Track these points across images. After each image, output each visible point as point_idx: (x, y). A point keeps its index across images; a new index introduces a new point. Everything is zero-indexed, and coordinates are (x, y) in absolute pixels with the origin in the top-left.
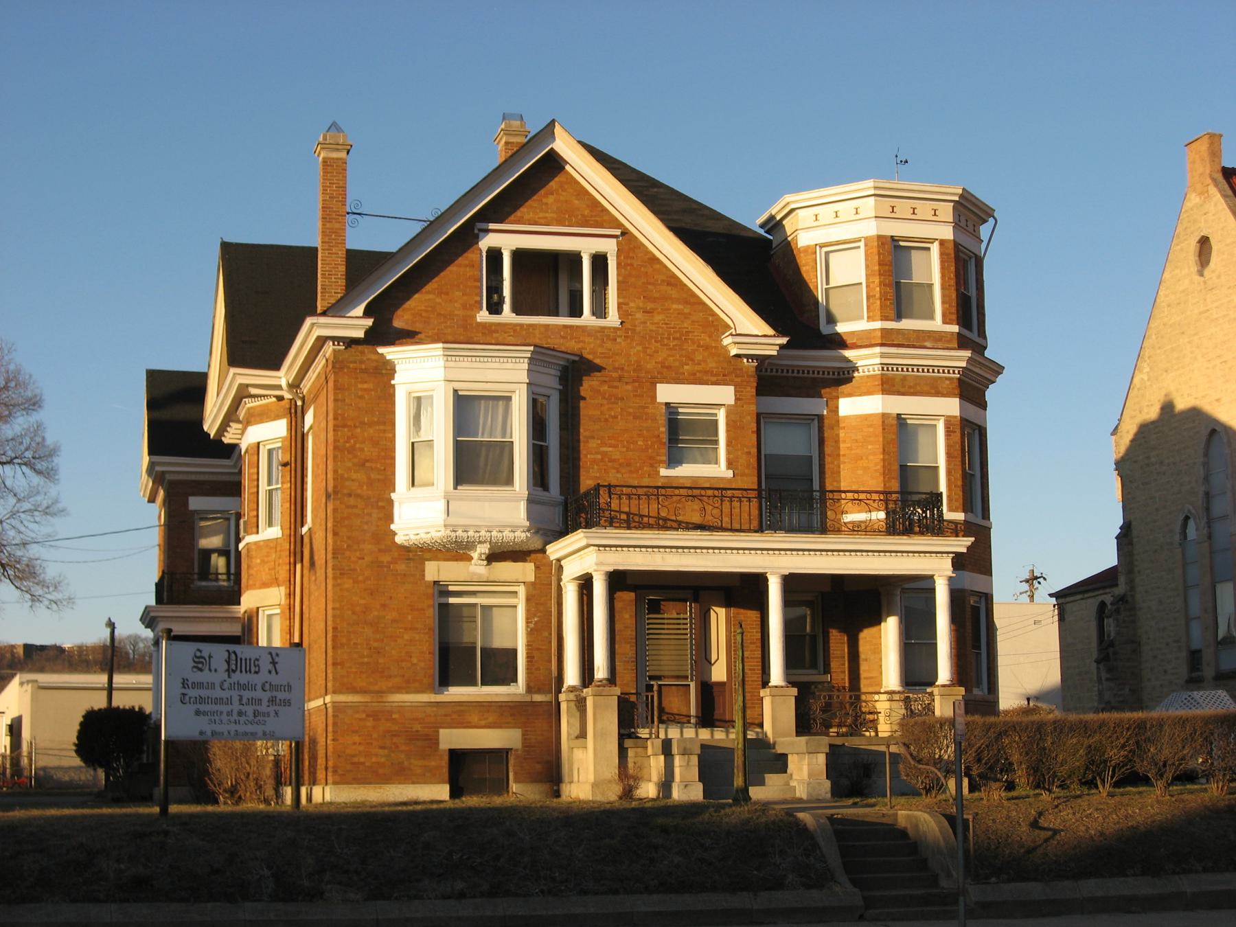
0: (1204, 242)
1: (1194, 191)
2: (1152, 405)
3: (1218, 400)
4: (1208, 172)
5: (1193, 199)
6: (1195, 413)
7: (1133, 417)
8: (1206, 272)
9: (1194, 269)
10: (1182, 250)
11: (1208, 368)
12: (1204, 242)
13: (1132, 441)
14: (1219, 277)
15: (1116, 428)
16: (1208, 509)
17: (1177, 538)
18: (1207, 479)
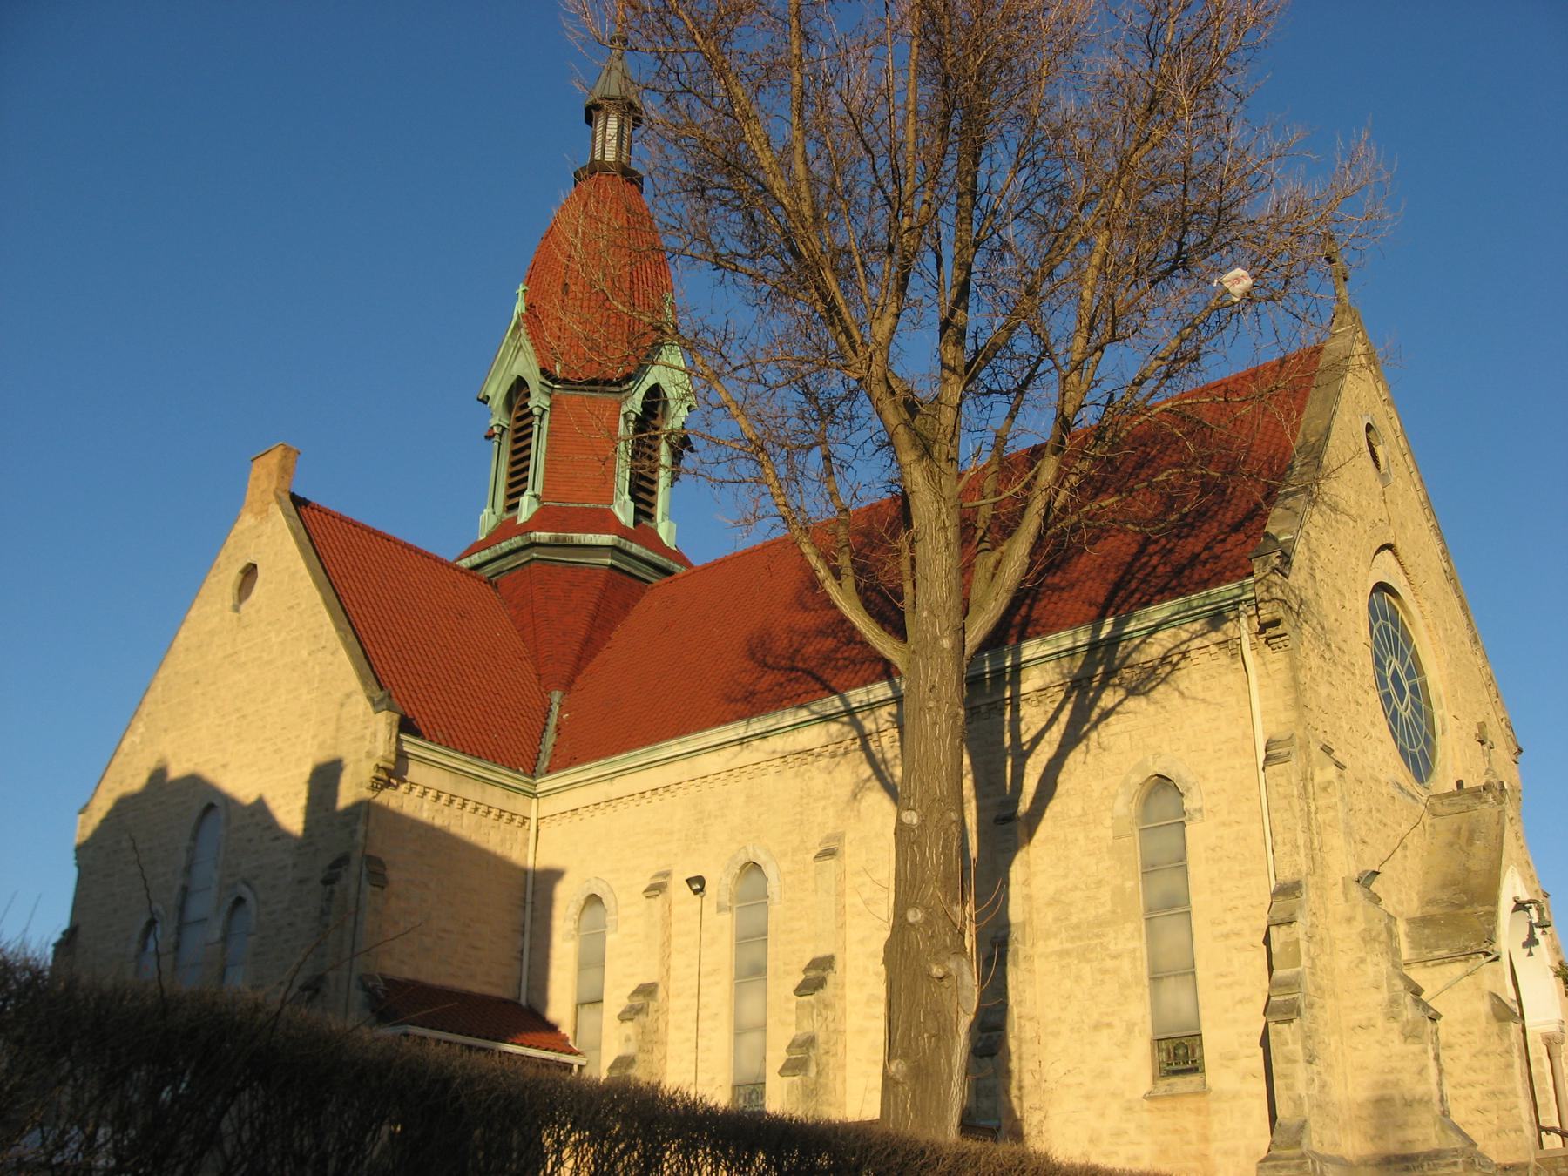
0: (250, 571)
1: (251, 512)
2: (138, 774)
3: (224, 766)
4: (273, 486)
5: (247, 520)
6: (194, 782)
7: (110, 790)
8: (244, 607)
9: (229, 603)
10: (219, 582)
11: (219, 725)
12: (250, 571)
13: (104, 821)
14: (258, 611)
15: (87, 806)
16: (182, 908)
17: (133, 948)
18: (188, 869)
